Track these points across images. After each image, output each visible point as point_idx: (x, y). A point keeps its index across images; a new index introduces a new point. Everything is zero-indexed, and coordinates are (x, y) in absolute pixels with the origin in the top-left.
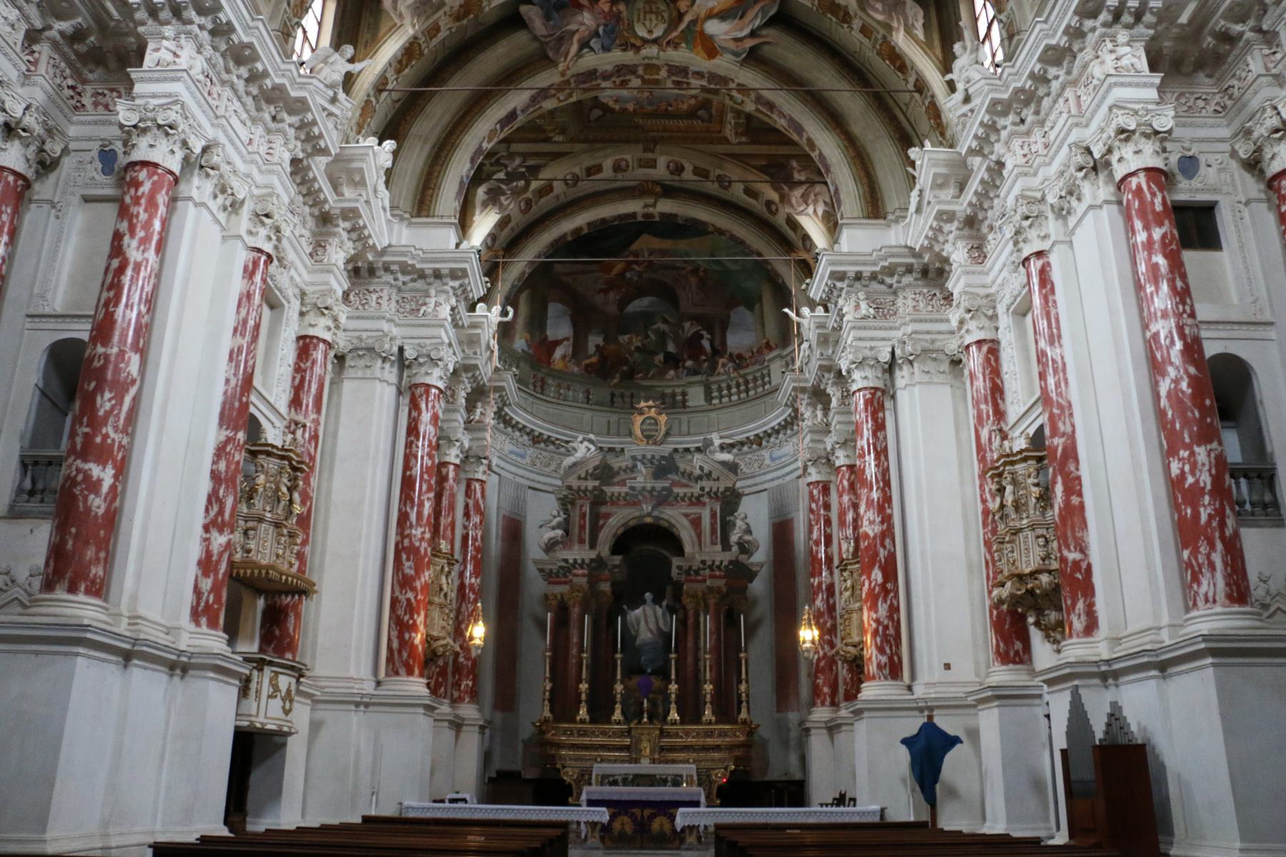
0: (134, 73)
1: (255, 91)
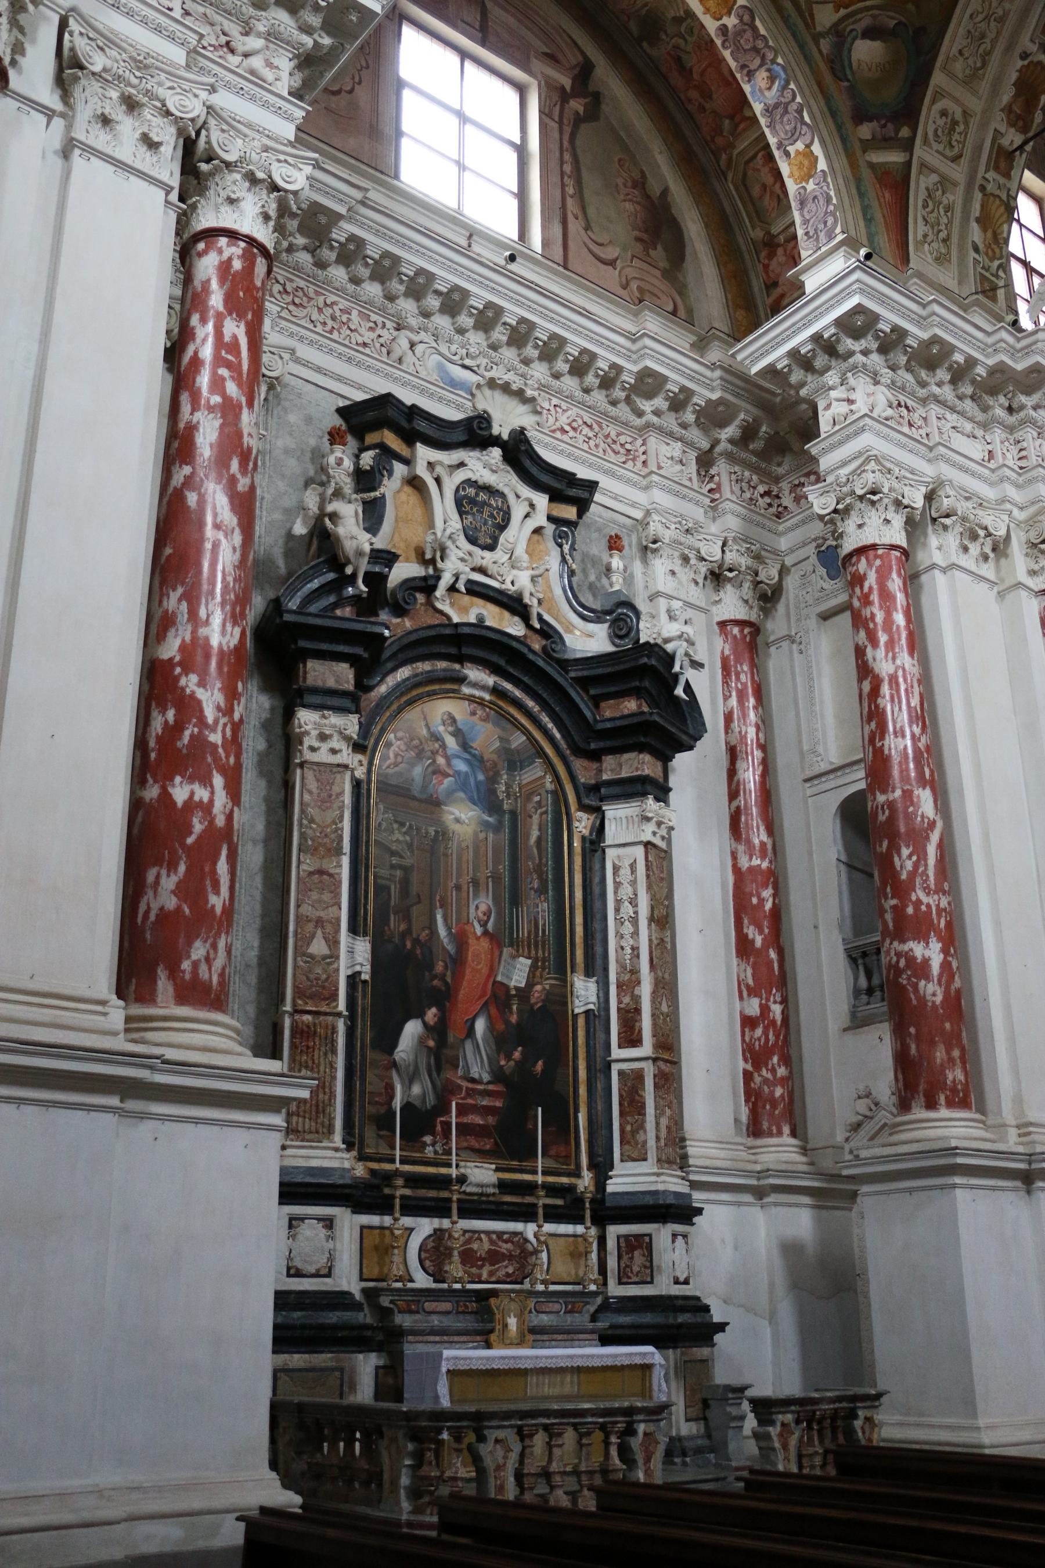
0: (813, 448)
1: (968, 390)
